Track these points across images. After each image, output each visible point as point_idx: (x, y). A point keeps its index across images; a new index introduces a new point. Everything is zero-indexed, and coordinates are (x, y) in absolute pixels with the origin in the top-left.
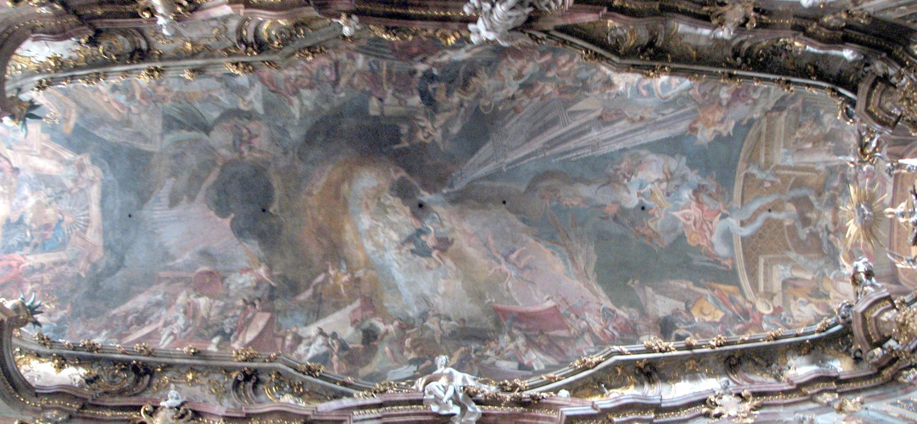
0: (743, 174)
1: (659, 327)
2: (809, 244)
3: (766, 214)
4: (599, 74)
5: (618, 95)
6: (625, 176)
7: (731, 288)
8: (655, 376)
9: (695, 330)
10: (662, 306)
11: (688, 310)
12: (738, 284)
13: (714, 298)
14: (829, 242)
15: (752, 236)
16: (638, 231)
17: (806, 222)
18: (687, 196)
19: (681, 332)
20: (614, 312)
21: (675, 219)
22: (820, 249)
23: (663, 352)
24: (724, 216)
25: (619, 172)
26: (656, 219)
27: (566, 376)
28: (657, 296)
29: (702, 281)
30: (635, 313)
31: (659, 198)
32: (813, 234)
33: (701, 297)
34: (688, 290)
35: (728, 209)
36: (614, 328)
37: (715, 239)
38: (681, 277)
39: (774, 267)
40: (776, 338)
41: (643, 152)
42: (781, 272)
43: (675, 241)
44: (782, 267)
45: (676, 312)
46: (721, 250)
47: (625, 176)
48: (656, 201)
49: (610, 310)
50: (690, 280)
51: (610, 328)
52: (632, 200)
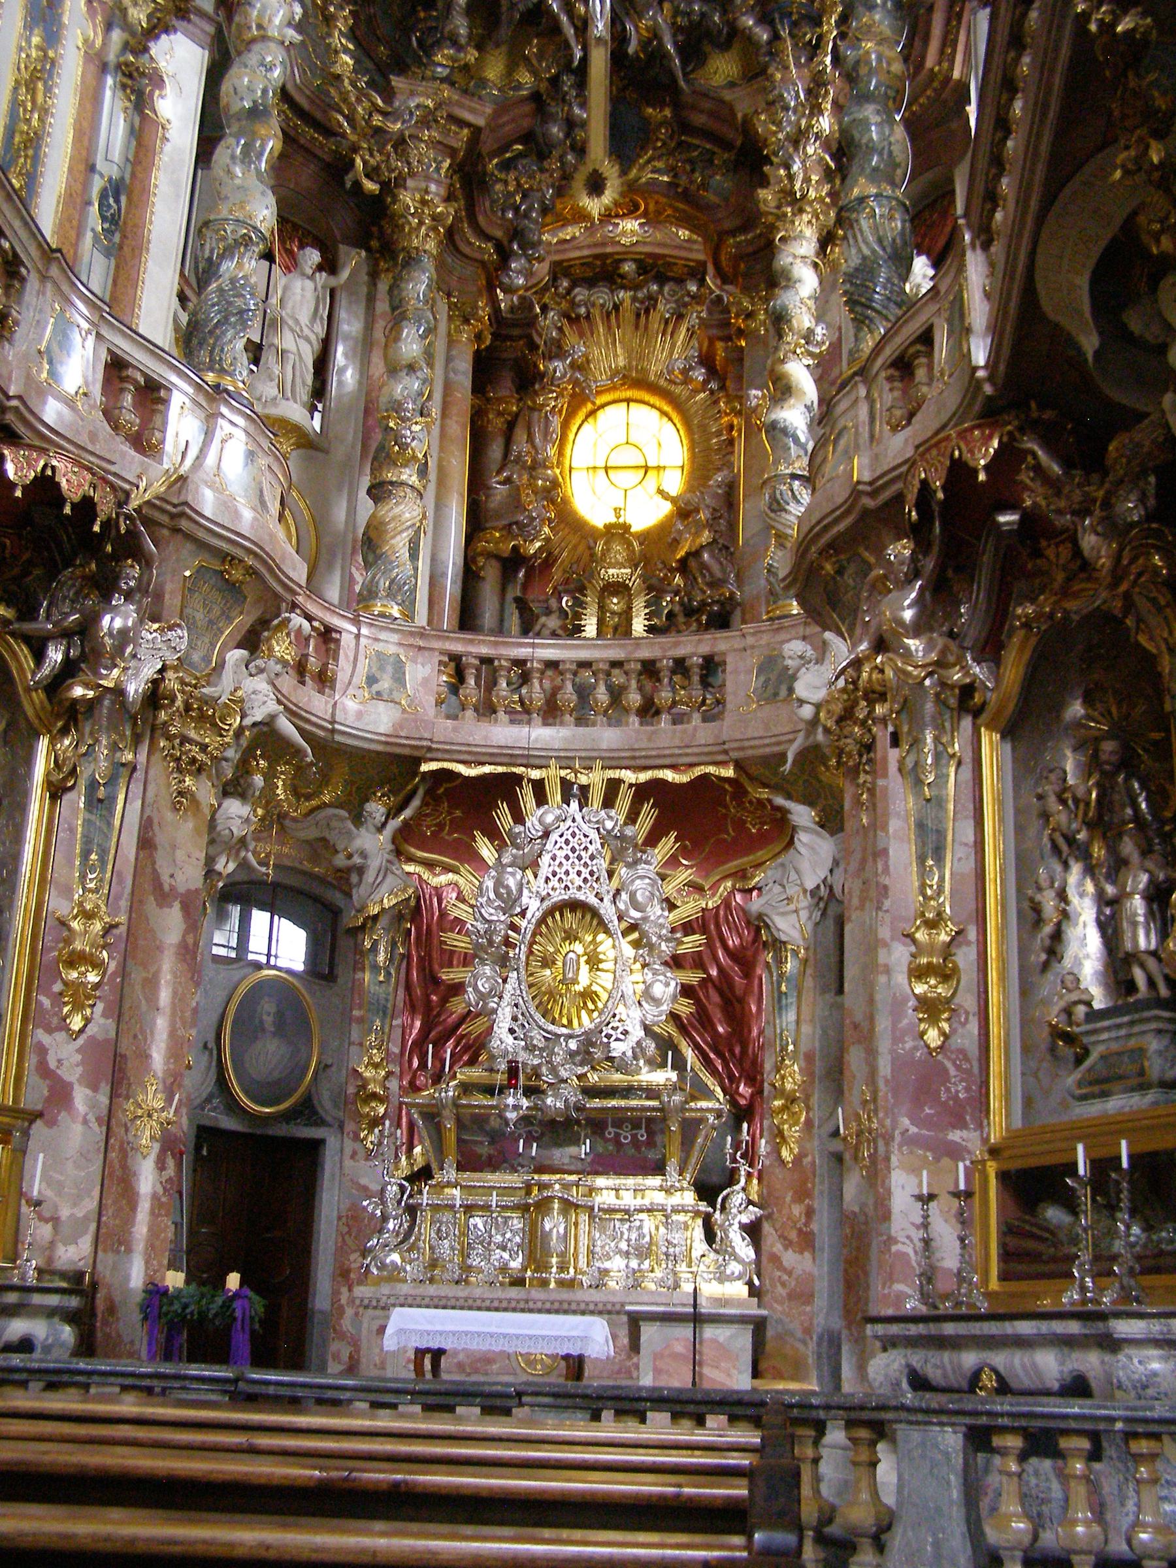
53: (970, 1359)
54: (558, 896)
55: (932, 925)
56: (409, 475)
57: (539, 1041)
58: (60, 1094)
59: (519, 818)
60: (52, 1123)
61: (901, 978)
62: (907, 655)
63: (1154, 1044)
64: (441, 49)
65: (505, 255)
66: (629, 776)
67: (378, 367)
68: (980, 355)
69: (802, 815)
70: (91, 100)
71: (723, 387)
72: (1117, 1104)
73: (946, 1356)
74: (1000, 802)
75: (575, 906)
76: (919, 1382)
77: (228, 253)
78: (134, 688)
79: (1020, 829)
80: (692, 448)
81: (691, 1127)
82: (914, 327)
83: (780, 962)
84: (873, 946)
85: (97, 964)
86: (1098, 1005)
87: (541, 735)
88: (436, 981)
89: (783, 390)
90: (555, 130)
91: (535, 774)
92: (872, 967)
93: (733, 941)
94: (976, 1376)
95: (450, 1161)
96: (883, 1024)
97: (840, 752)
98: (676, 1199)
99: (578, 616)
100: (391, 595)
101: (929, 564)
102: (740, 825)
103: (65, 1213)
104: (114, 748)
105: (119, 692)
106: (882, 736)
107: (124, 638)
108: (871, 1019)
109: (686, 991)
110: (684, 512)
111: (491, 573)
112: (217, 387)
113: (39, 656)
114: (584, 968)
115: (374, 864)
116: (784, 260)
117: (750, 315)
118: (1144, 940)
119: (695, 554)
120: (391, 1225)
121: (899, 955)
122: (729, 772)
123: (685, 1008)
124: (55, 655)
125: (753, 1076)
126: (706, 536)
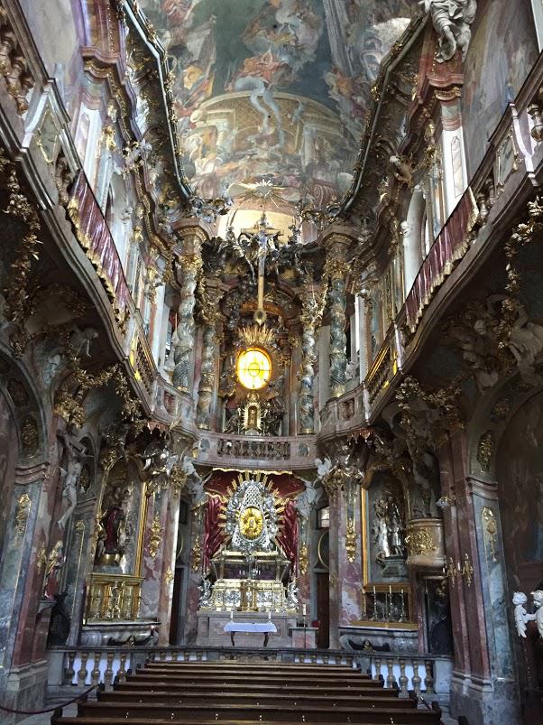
0: (298, 100)
1: (177, 44)
2: (243, 142)
3: (267, 114)
4: (388, 14)
5: (370, 22)
6: (302, 14)
7: (210, 91)
8: (144, 83)
9: (177, 72)
10: (195, 44)
11: (192, 63)
12: (212, 96)
13: (202, 80)
14: (244, 156)
15: (250, 104)
16: (256, 22)
17: (260, 141)
18: (283, 59)
19: (175, 62)
20: (189, 7)
21: (266, 50)
22: (239, 149)
23: (165, 88)
24: (266, 85)
25: (306, 10)
26: (266, 37)
27: (138, 19)
28: (203, 39)
29: (216, 70)
30: (188, 25)
31: (284, 39)
32: (250, 145)
33: (204, 71)
34: (208, 61)
35: (271, 88)
36: (176, 10)
37: (249, 78)
38: (219, 54)
39: (226, 120)
40: (177, 155)
41: (321, 31)
42: (222, 124)
43: (248, 51)
44: (225, 125)
45: (191, 55)
46: (240, 83)
47: (302, 14)
48: (280, 37)
49: (190, 4)
50: (217, 61)
51: (175, 8)
52: (282, 18)
53: (363, 638)
54: (248, 506)
55: (350, 534)
56: (209, 389)
57: (244, 544)
58: (150, 572)
59: (238, 485)
60: (148, 580)
61: (344, 545)
62: (346, 472)
63: (400, 567)
64: (216, 269)
65: (229, 319)
66: (266, 473)
67: (199, 355)
68: (367, 417)
69: (308, 483)
70: (143, 303)
71: (282, 349)
72: (391, 579)
73: (357, 637)
74: (365, 505)
75: (253, 507)
76: (350, 642)
77: (184, 355)
78: (168, 472)
79: (370, 511)
80: (272, 365)
81: (282, 567)
82: (351, 397)
83: (302, 521)
84: (337, 537)
85: (158, 539)
86: (388, 555)
87: (243, 461)
88: (212, 523)
89: (305, 372)
90: (244, 287)
91: (242, 471)
92: (337, 543)
93: (289, 514)
94: (364, 643)
95: (221, 576)
96: (340, 556)
97: (328, 488)
98: (277, 586)
99: (242, 415)
100: (205, 423)
101: (351, 451)
102: (292, 485)
103: (151, 602)
104: (162, 485)
105: (165, 473)
106: (340, 488)
107: (166, 459)
108: (337, 553)
109: (280, 530)
110: (269, 385)
111: (220, 402)
112: (183, 392)
113: (145, 463)
114: (255, 524)
115: (199, 493)
116: (305, 336)
117: (294, 342)
118: (398, 543)
119: (274, 398)
120: (206, 594)
121: (343, 540)
122: (291, 473)
123: (280, 534)
124: (148, 462)
125: (295, 551)
126: (277, 394)
